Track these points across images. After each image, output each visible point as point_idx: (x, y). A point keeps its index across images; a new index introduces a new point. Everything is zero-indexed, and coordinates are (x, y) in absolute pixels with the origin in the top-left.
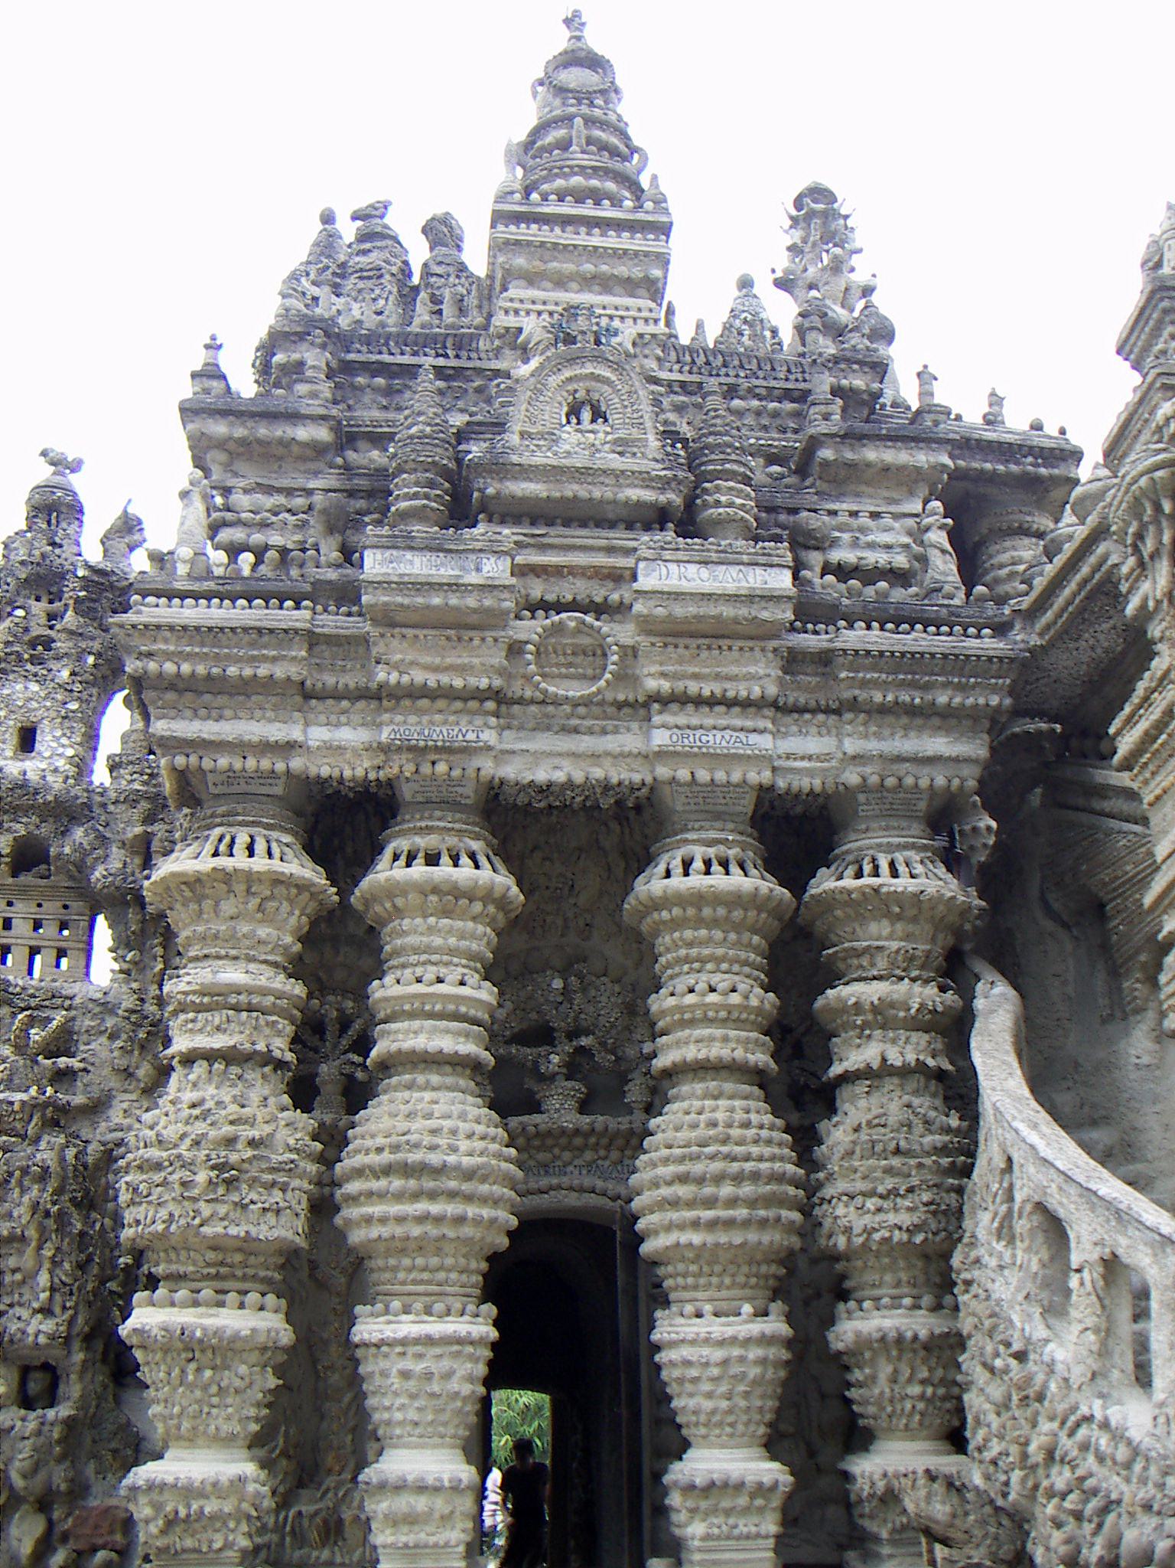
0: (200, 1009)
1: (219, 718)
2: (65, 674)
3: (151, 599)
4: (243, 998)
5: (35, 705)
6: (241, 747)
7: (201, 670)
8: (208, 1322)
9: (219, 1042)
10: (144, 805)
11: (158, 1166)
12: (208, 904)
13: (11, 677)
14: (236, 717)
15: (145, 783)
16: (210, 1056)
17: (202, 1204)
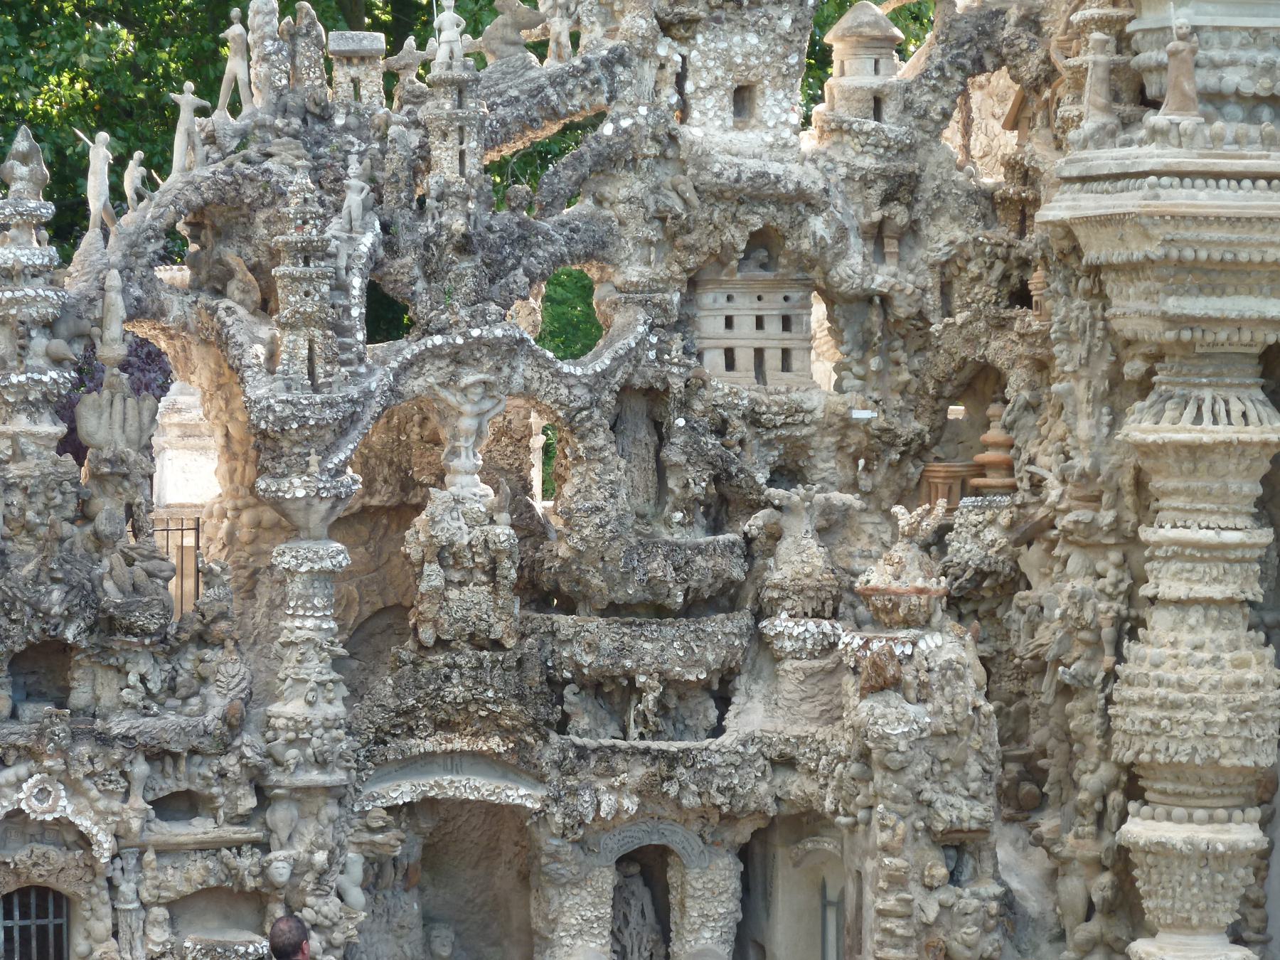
0: (1192, 559)
1: (1223, 293)
2: (787, 22)
3: (1165, 180)
4: (1239, 554)
5: (753, 61)
6: (1238, 324)
7: (1216, 256)
8: (1225, 837)
9: (1217, 592)
10: (881, 186)
11: (1176, 706)
12: (1202, 466)
13: (726, 27)
14: (1237, 292)
15: (878, 157)
16: (1208, 603)
17: (1221, 740)
